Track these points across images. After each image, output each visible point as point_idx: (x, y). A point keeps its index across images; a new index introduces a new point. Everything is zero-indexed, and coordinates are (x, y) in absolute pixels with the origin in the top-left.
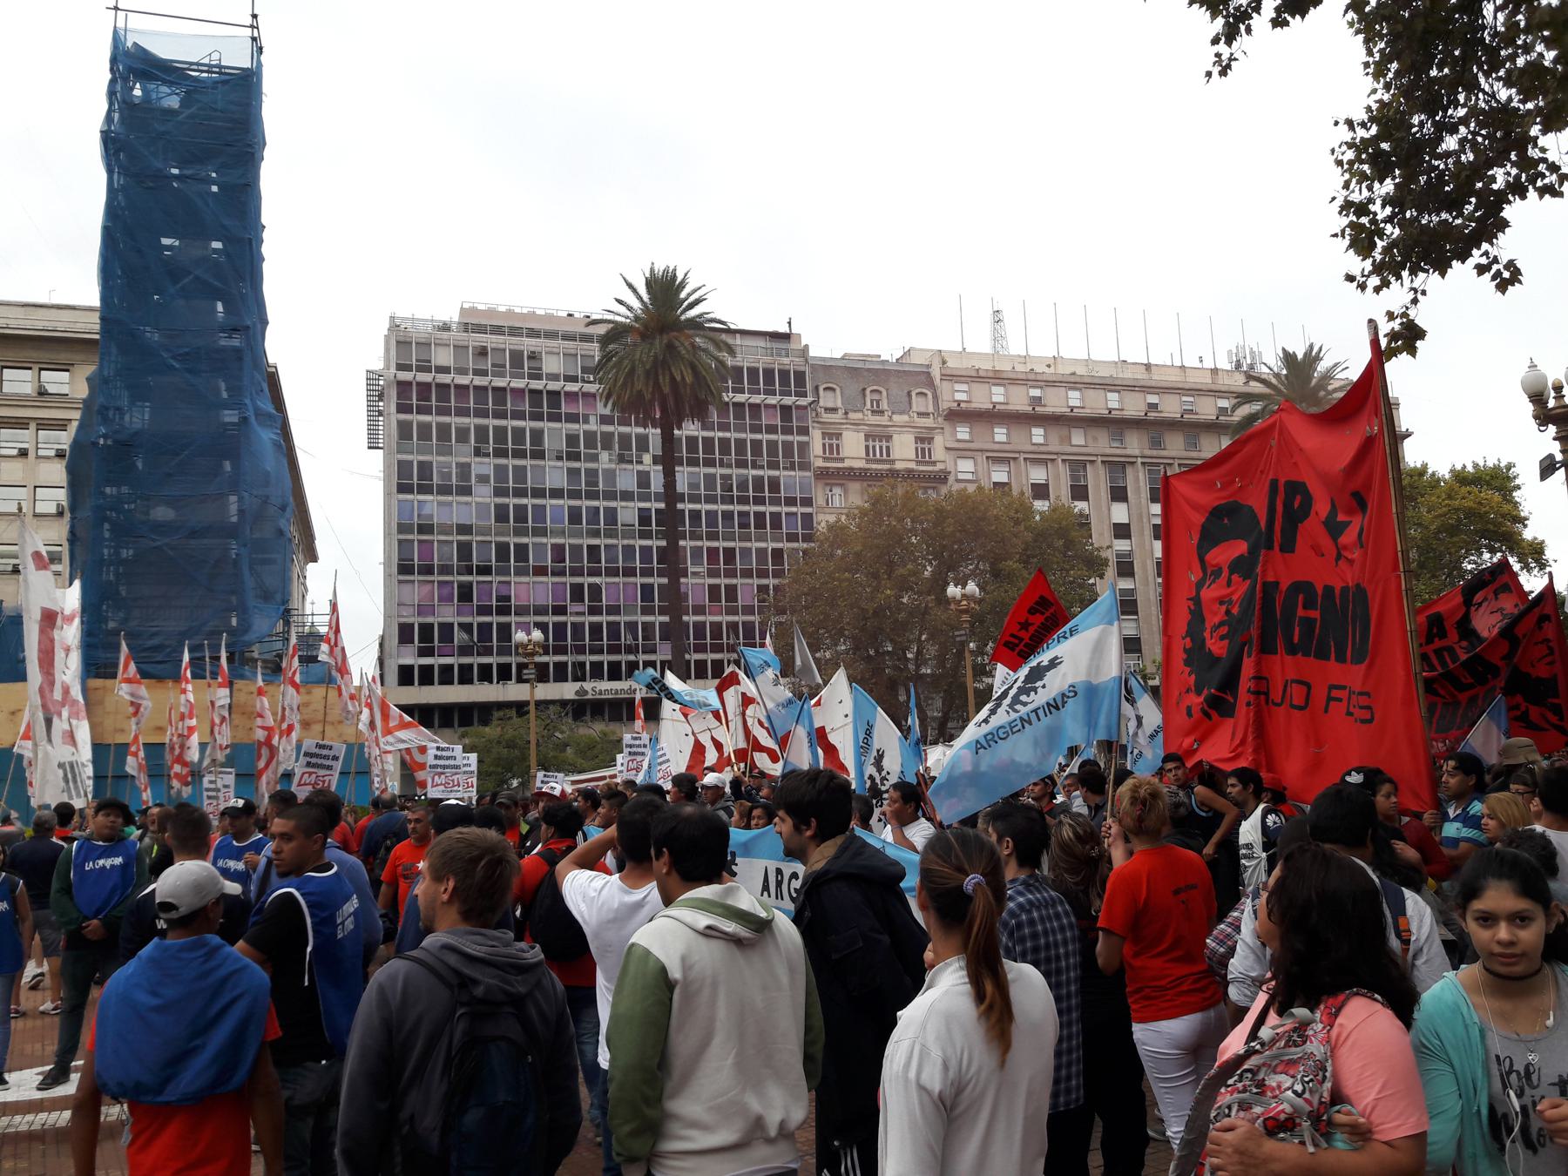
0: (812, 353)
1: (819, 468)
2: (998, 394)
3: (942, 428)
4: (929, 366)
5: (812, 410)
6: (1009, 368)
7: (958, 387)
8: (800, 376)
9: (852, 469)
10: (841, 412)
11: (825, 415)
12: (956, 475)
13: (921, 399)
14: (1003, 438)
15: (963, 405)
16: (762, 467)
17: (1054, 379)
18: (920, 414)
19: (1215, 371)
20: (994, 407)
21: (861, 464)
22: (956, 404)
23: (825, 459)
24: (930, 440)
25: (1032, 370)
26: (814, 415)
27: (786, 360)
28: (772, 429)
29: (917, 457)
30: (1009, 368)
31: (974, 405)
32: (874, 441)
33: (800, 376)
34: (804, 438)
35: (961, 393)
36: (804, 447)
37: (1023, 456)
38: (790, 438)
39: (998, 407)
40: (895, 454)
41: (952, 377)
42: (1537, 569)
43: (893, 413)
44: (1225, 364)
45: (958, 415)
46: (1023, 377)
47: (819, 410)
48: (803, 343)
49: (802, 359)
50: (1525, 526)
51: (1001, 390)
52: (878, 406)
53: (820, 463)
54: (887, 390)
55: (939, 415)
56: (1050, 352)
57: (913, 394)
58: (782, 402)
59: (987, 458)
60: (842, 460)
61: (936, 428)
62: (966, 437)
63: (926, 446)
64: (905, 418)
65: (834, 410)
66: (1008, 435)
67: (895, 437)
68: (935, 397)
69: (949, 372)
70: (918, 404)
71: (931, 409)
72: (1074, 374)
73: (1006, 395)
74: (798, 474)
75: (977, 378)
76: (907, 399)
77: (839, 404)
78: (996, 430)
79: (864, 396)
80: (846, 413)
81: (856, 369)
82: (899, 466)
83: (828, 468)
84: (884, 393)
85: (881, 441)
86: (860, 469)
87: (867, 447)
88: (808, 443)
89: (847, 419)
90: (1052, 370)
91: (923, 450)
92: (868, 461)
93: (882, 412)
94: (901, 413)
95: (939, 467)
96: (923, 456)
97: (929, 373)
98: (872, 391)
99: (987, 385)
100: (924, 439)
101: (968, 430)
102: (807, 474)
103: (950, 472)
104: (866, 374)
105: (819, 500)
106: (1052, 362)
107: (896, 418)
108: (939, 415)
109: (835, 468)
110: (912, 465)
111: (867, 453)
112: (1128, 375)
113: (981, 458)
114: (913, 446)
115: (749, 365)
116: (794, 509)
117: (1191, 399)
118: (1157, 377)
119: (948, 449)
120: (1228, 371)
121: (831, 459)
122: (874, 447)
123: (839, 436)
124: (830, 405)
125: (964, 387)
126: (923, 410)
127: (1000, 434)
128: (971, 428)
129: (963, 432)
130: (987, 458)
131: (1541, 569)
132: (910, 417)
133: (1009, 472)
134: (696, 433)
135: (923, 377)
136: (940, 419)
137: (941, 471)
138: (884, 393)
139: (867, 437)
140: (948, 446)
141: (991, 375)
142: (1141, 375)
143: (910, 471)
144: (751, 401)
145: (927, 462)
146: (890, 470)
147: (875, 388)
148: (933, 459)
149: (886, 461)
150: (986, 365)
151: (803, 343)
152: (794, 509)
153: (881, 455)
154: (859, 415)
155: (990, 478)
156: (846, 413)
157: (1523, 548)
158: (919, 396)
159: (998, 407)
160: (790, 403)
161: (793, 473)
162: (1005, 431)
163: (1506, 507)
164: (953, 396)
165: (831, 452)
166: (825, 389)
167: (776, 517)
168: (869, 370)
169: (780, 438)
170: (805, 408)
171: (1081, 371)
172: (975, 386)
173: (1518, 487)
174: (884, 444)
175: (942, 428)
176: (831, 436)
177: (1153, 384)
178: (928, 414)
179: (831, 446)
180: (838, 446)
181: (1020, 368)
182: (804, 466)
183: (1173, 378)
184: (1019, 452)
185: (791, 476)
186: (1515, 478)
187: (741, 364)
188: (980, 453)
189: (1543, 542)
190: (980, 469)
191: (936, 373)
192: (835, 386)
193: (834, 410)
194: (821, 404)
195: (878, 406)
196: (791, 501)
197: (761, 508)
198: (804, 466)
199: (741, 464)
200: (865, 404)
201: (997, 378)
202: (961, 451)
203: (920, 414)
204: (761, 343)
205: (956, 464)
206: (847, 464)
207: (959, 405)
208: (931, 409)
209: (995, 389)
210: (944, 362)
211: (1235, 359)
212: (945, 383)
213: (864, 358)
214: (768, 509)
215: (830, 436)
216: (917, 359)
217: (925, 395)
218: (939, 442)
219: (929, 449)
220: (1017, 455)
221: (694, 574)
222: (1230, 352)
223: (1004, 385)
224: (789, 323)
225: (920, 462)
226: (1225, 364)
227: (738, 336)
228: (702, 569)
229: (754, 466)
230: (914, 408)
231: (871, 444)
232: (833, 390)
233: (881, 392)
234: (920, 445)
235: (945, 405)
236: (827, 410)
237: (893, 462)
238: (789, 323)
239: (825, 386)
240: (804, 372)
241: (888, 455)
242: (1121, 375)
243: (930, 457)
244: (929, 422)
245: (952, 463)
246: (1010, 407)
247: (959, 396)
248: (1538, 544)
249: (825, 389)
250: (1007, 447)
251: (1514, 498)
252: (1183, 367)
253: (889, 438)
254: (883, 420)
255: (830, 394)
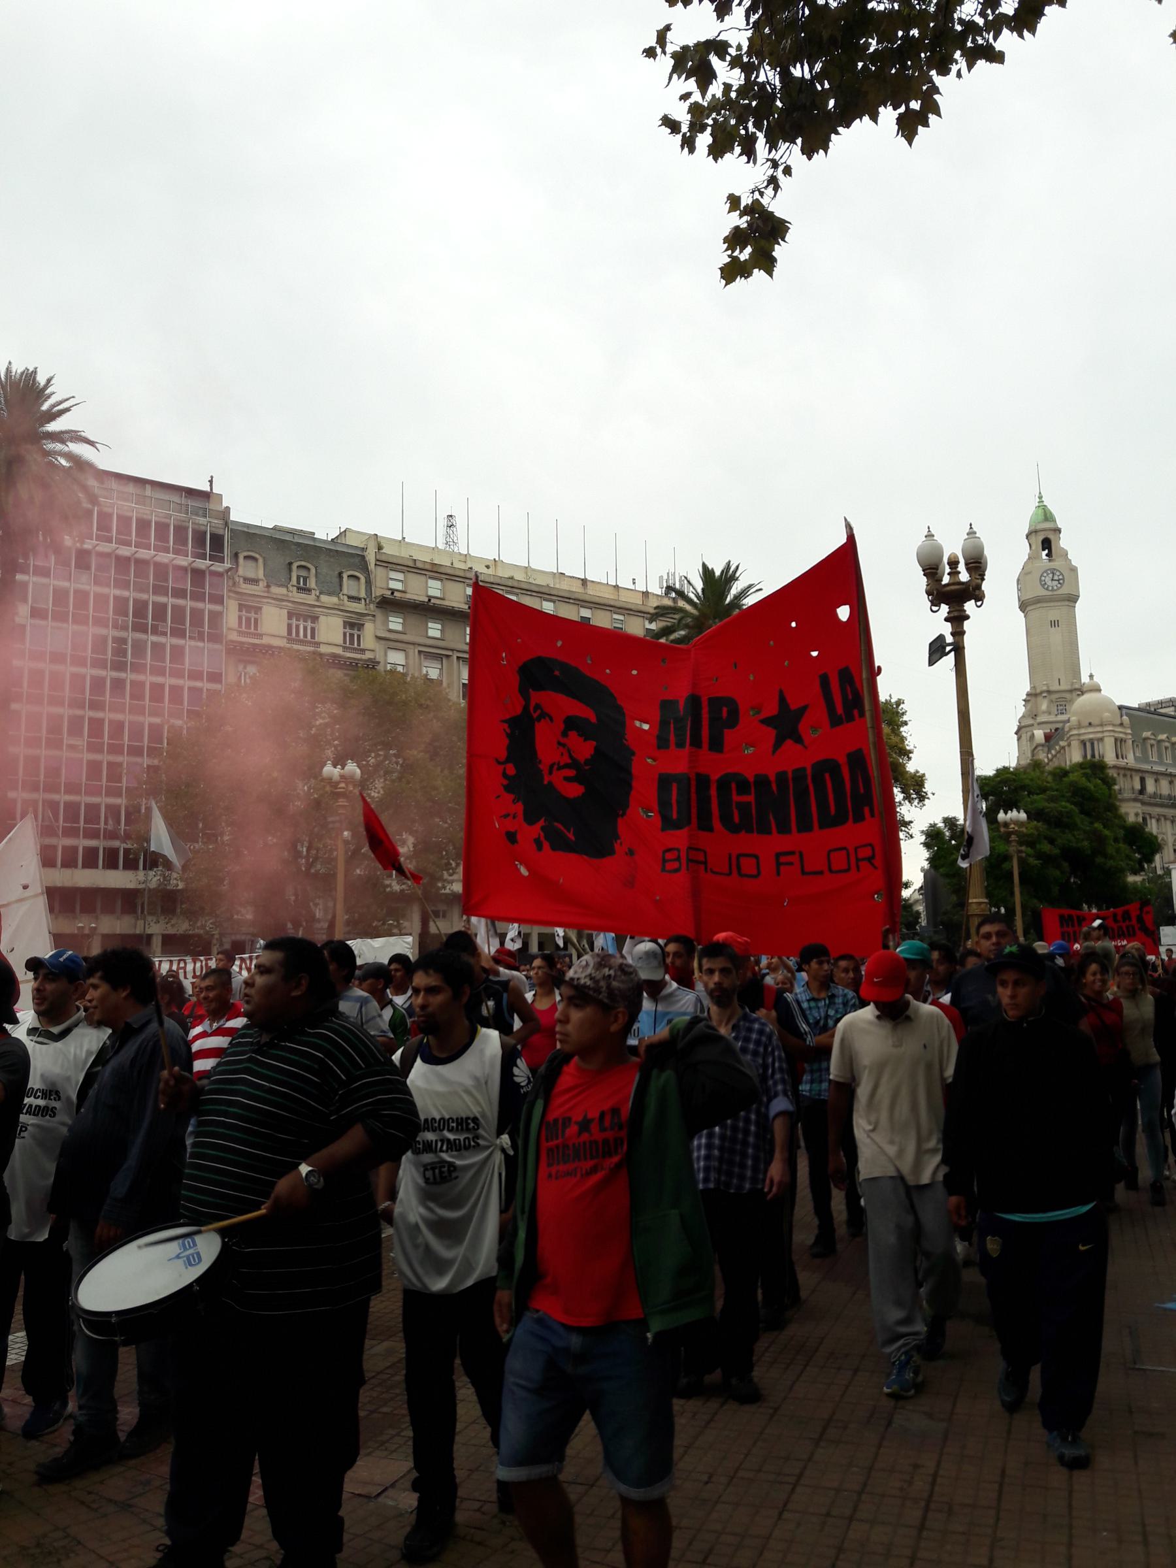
0: (234, 517)
1: (232, 641)
2: (434, 588)
3: (374, 616)
4: (363, 549)
5: (229, 578)
6: (449, 565)
7: (393, 575)
8: (217, 541)
9: (270, 647)
10: (262, 584)
11: (244, 586)
12: (386, 666)
13: (352, 582)
14: (437, 634)
15: (396, 594)
16: (165, 634)
17: (492, 580)
18: (351, 598)
19: (646, 594)
20: (429, 600)
21: (282, 643)
22: (389, 593)
23: (240, 633)
24: (360, 627)
25: (471, 568)
26: (231, 583)
27: (202, 520)
28: (180, 593)
29: (345, 642)
30: (449, 565)
31: (408, 596)
32: (298, 620)
33: (217, 541)
34: (218, 608)
35: (396, 582)
36: (216, 617)
37: (456, 654)
38: (200, 605)
39: (433, 601)
40: (322, 636)
41: (388, 564)
42: (917, 801)
43: (320, 593)
44: (656, 589)
45: (390, 604)
46: (461, 574)
47: (237, 579)
48: (225, 504)
49: (221, 522)
50: (910, 759)
51: (437, 584)
52: (305, 583)
53: (234, 636)
54: (316, 568)
55: (371, 602)
56: (491, 555)
57: (345, 576)
58: (194, 565)
59: (420, 652)
60: (260, 636)
61: (368, 615)
62: (399, 628)
63: (356, 632)
64: (334, 600)
65: (255, 581)
66: (442, 631)
67: (322, 619)
68: (369, 583)
69: (383, 558)
70: (349, 587)
71: (363, 594)
72: (512, 578)
73: (443, 590)
74: (206, 645)
75: (413, 568)
76: (337, 580)
77: (261, 574)
78: (430, 625)
79: (290, 570)
80: (268, 586)
81: (283, 541)
82: (324, 649)
83: (243, 643)
84: (313, 571)
85: (305, 621)
86: (280, 648)
87: (289, 627)
88: (220, 614)
89: (268, 592)
90: (490, 572)
91: (352, 635)
92: (290, 640)
93: (307, 590)
94: (330, 594)
95: (368, 655)
96: (352, 642)
97: (363, 557)
98: (298, 567)
99: (423, 578)
100: (354, 625)
101: (401, 620)
102: (217, 646)
103: (379, 663)
104: (293, 547)
105: (231, 679)
106: (491, 564)
107: (325, 599)
108: (371, 602)
109: (250, 644)
110: (339, 651)
111: (290, 632)
112: (564, 586)
113: (413, 652)
114: (341, 630)
115: (157, 519)
116: (198, 684)
117: (621, 617)
118: (591, 591)
119: (377, 637)
120: (658, 595)
121: (247, 633)
122: (297, 627)
123: (258, 610)
124: (251, 575)
125: (400, 576)
126: (354, 594)
127: (434, 629)
128: (404, 620)
129: (396, 623)
130: (420, 652)
131: (920, 801)
132: (339, 599)
133: (441, 669)
134: (87, 587)
135: (357, 560)
136: (372, 606)
137: (370, 660)
138: (313, 571)
139: (290, 615)
140: (379, 635)
141: (428, 567)
142: (576, 588)
143: (335, 656)
144: (158, 559)
145: (355, 649)
146: (314, 653)
147: (303, 563)
148: (362, 647)
149: (310, 642)
150: (425, 557)
151: (225, 504)
152: (198, 684)
153: (305, 635)
154: (283, 591)
155: (420, 670)
156: (268, 586)
157: (907, 779)
158: (352, 578)
159: (433, 601)
160: (203, 567)
161: (201, 644)
162: (439, 626)
163: (894, 739)
164: (388, 584)
165: (248, 626)
166: (246, 557)
167: (176, 691)
168: (298, 544)
169: (188, 604)
170: (220, 575)
171: (520, 576)
172: (410, 575)
173: (906, 723)
174: (309, 625)
175: (374, 616)
176: (251, 610)
177: (587, 598)
178: (360, 599)
179: (248, 620)
180: (256, 620)
181: (457, 565)
182: (215, 638)
183: (608, 596)
184: (452, 650)
185: (197, 647)
186: (903, 714)
187: (150, 517)
188: (412, 646)
189: (924, 775)
190: (411, 662)
191: (371, 558)
192: (257, 556)
193: (255, 581)
194: (241, 572)
195: (305, 583)
196: (195, 675)
197: (159, 680)
198: (215, 638)
199: (141, 628)
200: (290, 579)
201: (434, 571)
202: (390, 641)
203: (351, 598)
204: (175, 498)
205: (386, 655)
206: (266, 640)
207: (392, 593)
208: (363, 594)
209: (431, 583)
210: (380, 548)
211: (665, 585)
212: (380, 569)
213: (293, 532)
214: (169, 681)
215: (249, 609)
216: (351, 541)
217: (357, 578)
218: (369, 628)
219: (359, 636)
220: (450, 653)
221: (72, 747)
222: (661, 578)
223: (441, 580)
224: (211, 482)
225: (347, 648)
226: (656, 589)
227: (148, 487)
228: (82, 742)
229: (155, 631)
230: (345, 591)
231: (294, 622)
232: (255, 559)
233: (309, 569)
234: (348, 631)
235: (378, 592)
236: (248, 580)
237: (318, 644)
238: (211, 482)
239: (246, 554)
240: (223, 536)
241: (313, 636)
242: (557, 586)
243: (359, 644)
244: (359, 607)
245: (382, 653)
246: (446, 603)
247: (394, 585)
248: (919, 777)
249: (246, 557)
250: (440, 644)
251: (901, 732)
252: (616, 587)
253: (315, 619)
254: (310, 599)
255: (251, 563)
